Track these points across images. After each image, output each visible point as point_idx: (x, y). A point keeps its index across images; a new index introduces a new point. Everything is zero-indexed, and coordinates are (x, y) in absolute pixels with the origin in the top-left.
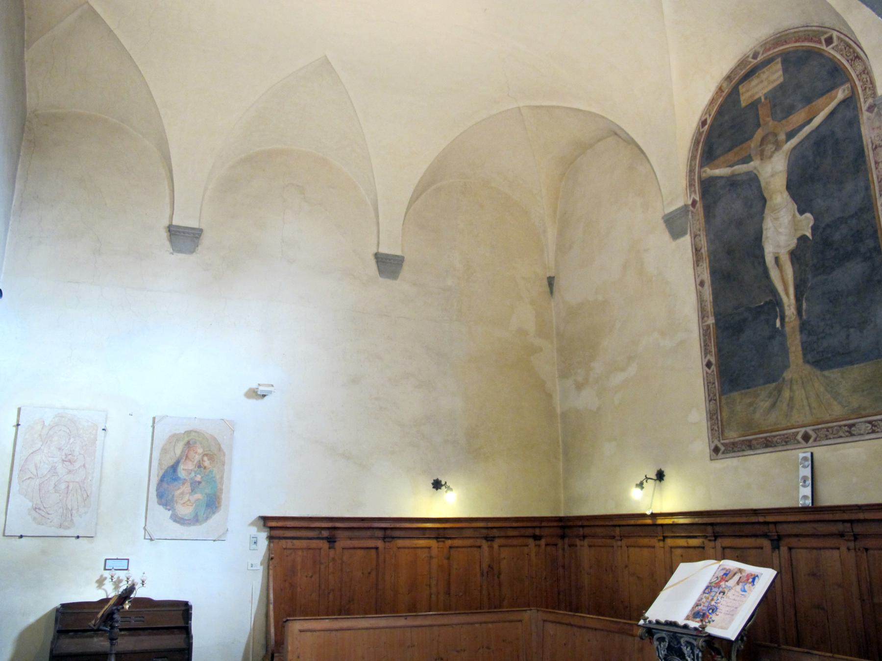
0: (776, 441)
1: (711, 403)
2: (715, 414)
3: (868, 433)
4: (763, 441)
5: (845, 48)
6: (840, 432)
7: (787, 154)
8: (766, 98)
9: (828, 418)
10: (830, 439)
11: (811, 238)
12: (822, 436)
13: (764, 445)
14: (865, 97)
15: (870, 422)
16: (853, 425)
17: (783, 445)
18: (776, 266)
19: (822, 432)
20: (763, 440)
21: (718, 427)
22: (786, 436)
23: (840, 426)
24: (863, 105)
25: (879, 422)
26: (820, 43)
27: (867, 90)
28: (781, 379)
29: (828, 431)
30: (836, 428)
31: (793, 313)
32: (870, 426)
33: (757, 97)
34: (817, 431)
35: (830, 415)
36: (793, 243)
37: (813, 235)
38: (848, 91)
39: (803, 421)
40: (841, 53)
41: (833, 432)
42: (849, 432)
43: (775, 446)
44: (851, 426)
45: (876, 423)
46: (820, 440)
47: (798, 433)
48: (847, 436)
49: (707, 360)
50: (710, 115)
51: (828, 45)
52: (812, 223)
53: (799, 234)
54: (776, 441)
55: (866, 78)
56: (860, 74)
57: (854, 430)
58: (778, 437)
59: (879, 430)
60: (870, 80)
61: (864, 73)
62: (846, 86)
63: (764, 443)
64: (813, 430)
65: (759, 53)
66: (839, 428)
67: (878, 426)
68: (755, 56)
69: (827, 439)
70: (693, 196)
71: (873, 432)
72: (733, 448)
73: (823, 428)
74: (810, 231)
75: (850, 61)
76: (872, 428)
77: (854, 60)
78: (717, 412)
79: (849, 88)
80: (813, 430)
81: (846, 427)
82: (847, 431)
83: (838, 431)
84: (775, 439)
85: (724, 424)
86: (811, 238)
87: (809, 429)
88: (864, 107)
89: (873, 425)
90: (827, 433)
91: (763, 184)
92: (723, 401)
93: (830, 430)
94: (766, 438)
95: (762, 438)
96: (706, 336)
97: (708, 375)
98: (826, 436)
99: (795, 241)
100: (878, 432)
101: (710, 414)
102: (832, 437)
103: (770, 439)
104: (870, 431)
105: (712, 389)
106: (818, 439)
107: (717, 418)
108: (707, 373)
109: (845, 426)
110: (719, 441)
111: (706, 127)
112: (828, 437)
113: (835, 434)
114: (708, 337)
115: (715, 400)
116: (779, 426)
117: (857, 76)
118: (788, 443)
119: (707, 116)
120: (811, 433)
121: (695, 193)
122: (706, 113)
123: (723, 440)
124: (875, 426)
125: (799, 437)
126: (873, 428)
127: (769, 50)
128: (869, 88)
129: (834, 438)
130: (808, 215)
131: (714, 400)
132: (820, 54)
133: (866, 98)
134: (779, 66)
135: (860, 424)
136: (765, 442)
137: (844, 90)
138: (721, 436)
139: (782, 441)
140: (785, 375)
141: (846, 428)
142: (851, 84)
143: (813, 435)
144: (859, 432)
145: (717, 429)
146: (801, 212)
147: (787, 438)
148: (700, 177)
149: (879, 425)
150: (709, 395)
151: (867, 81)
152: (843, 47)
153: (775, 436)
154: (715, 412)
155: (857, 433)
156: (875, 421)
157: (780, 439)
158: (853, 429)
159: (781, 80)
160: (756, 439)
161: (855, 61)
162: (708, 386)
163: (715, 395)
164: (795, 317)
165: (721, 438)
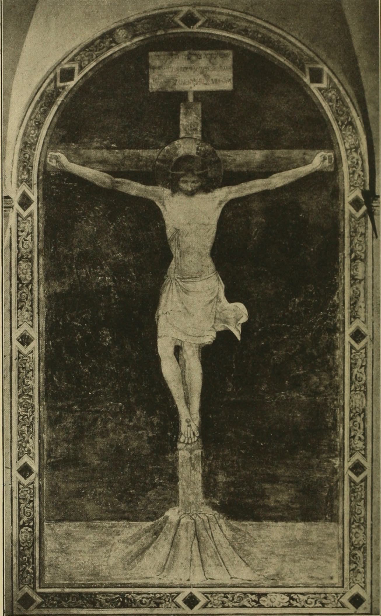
0: (141, 601)
1: (23, 530)
2: (29, 549)
3: (283, 607)
4: (116, 598)
5: (337, 101)
6: (245, 600)
7: (220, 203)
8: (196, 99)
9: (229, 582)
10: (228, 607)
11: (239, 338)
12: (216, 602)
13: (119, 604)
14: (352, 184)
15: (289, 594)
16: (265, 594)
17: (151, 607)
18: (174, 359)
19: (216, 598)
20: (118, 596)
21: (34, 568)
22: (158, 596)
23: (245, 594)
24: (346, 192)
25: (299, 595)
26: (303, 69)
27: (356, 176)
28: (161, 519)
29: (227, 597)
30: (238, 594)
31: (194, 433)
32: (287, 599)
33: (179, 87)
34: (209, 596)
35: (231, 578)
36: (209, 338)
37: (242, 335)
38: (329, 162)
39: (189, 580)
40: (331, 104)
41: (233, 599)
42: (257, 602)
43: (138, 607)
44: (260, 595)
45: (295, 597)
46: (212, 607)
47: (178, 594)
48: (253, 607)
49: (21, 463)
50: (81, 68)
51: (313, 81)
52: (244, 319)
53: (220, 327)
54: (141, 601)
55: (357, 160)
56: (351, 149)
57: (264, 601)
58: (145, 596)
59: (298, 605)
60: (362, 164)
61: (356, 151)
62: (329, 154)
63: (118, 602)
64: (204, 593)
65: (196, 21)
66: (243, 596)
67: (298, 600)
68: (189, 20)
69: (224, 607)
70: (24, 187)
71: (290, 606)
72: (59, 602)
73: (220, 593)
74: (239, 328)
75: (340, 123)
76: (289, 601)
77: (346, 127)
78: (33, 544)
79: (331, 159)
80: (204, 593)
81: (254, 596)
82: (255, 601)
83: (241, 599)
84: (139, 598)
85: (46, 563)
86: (239, 338)
87: (196, 592)
88: (349, 197)
89: (292, 598)
90: (225, 599)
91: (169, 232)
92: (47, 531)
93: (229, 596)
94: (122, 595)
95: (115, 593)
96: (24, 425)
97: (21, 486)
98: (223, 603)
99: (214, 335)
100: (296, 607)
101: (20, 546)
102: (231, 606)
103: (130, 597)
104: (286, 604)
105: (27, 510)
106: (209, 605)
107: (33, 555)
108: (19, 483)
109: (252, 594)
110: (34, 588)
111: (71, 84)
112: (226, 605)
113: (235, 602)
114: (29, 427)
115: (33, 527)
116: (150, 581)
117: (347, 150)
118: (160, 606)
119: (76, 66)
120: (199, 596)
121: (30, 186)
122: (73, 60)
123: (40, 587)
124: (293, 599)
125: (179, 600)
126: (291, 601)
127: (216, 26)
128: (359, 175)
129: (234, 607)
130: (241, 306)
131: (29, 526)
132: (302, 89)
133: (353, 186)
134: (229, 62)
135: (274, 594)
136: (121, 600)
137: (325, 159)
138: (37, 582)
139: (150, 601)
140: (167, 514)
141: (254, 597)
142: (335, 156)
143: (203, 601)
144: (271, 604)
145: (31, 571)
146: (231, 297)
147: (160, 598)
148: (44, 164)
149: (299, 599)
150: (20, 519)
151: (357, 164)
152: (334, 97)
153: (138, 594)
154: (30, 545)
155: (267, 605)
156: (295, 594)
157: (147, 598)
158: (263, 598)
159: (228, 86)
160: (104, 594)
161: (348, 127)
162: (20, 504)
163: (32, 519)
164: (196, 438)
165: (37, 585)
